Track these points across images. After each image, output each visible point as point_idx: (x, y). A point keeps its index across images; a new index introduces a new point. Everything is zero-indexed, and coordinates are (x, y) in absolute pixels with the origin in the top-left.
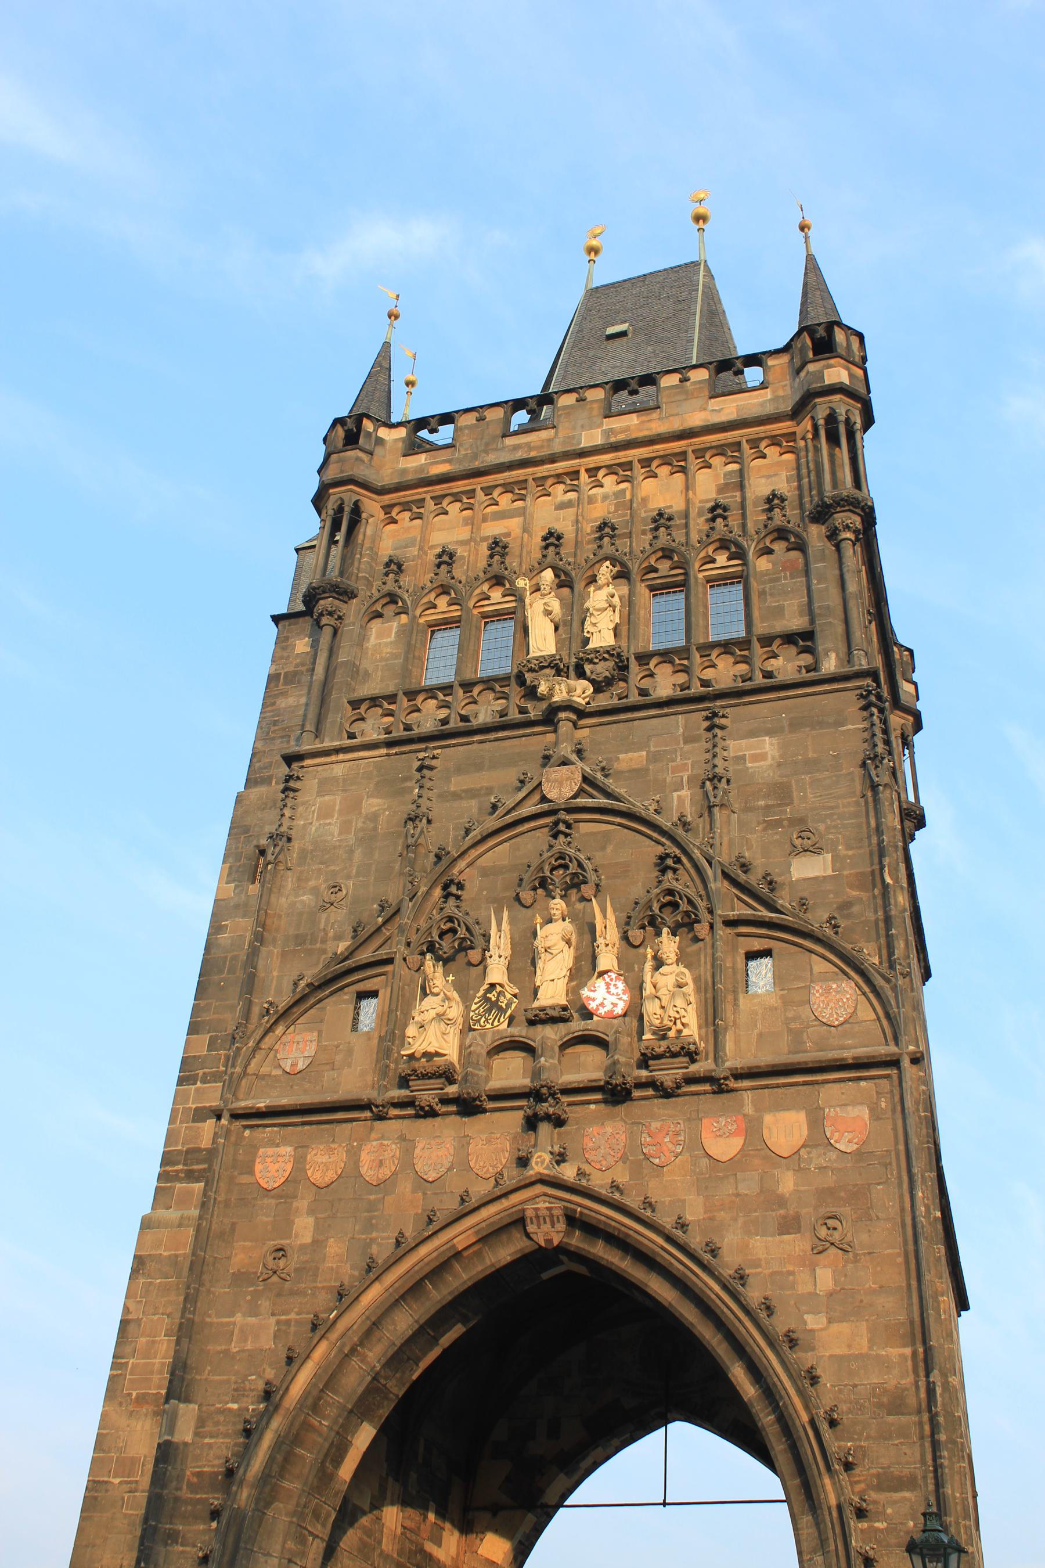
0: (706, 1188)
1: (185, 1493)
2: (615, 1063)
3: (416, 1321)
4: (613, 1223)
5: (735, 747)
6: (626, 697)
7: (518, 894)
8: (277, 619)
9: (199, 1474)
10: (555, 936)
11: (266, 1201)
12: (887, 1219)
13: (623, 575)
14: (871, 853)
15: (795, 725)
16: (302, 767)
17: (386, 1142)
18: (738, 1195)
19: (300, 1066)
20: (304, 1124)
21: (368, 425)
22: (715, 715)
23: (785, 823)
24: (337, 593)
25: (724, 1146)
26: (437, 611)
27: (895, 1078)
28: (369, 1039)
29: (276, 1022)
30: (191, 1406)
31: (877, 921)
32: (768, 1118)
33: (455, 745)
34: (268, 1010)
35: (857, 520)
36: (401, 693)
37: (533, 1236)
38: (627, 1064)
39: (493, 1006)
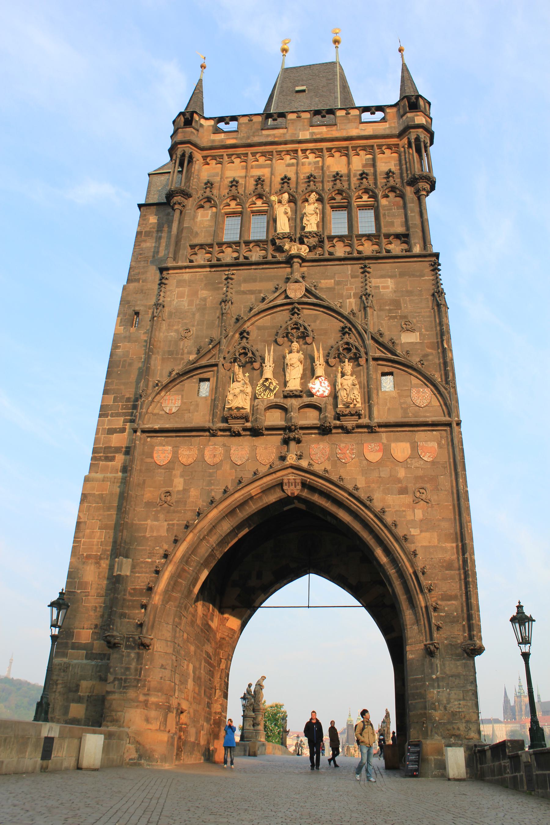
0: (366, 473)
1: (128, 597)
2: (326, 417)
3: (232, 526)
4: (324, 487)
5: (374, 282)
6: (323, 255)
7: (276, 339)
8: (140, 206)
9: (134, 589)
10: (295, 359)
11: (159, 470)
12: (446, 490)
13: (320, 200)
14: (437, 334)
15: (402, 275)
16: (168, 274)
18: (380, 477)
19: (174, 410)
20: (177, 436)
21: (196, 117)
22: (365, 266)
23: (398, 317)
24: (183, 194)
25: (374, 456)
26: (230, 207)
27: (449, 431)
28: (206, 400)
29: (161, 390)
30: (129, 560)
31: (440, 364)
32: (393, 445)
33: (243, 270)
34: (157, 385)
35: (428, 186)
36: (215, 243)
37: (286, 491)
38: (331, 418)
39: (267, 388)
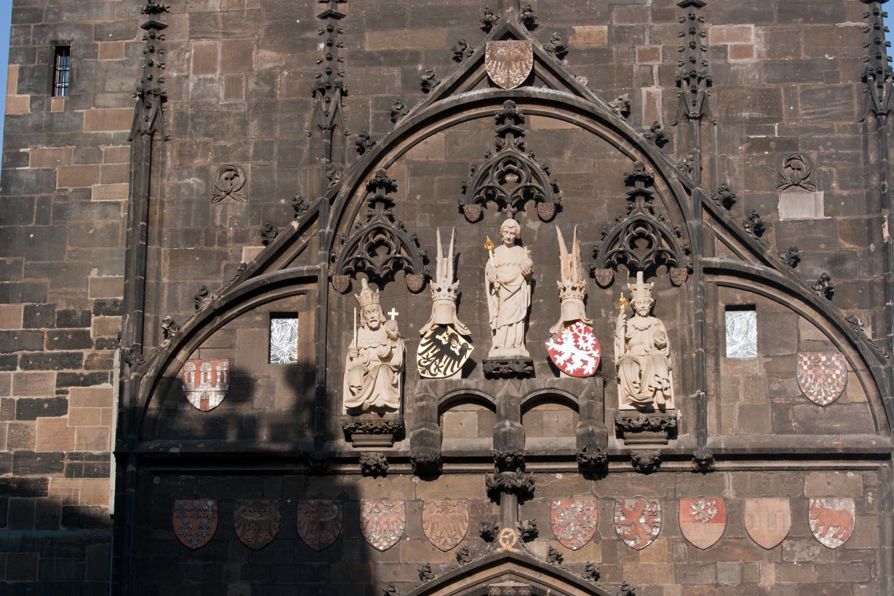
0: (685, 576)
5: (715, 33)
14: (869, 197)
17: (326, 502)
18: (717, 585)
20: (225, 473)
25: (704, 532)
32: (750, 505)
39: (445, 350)
